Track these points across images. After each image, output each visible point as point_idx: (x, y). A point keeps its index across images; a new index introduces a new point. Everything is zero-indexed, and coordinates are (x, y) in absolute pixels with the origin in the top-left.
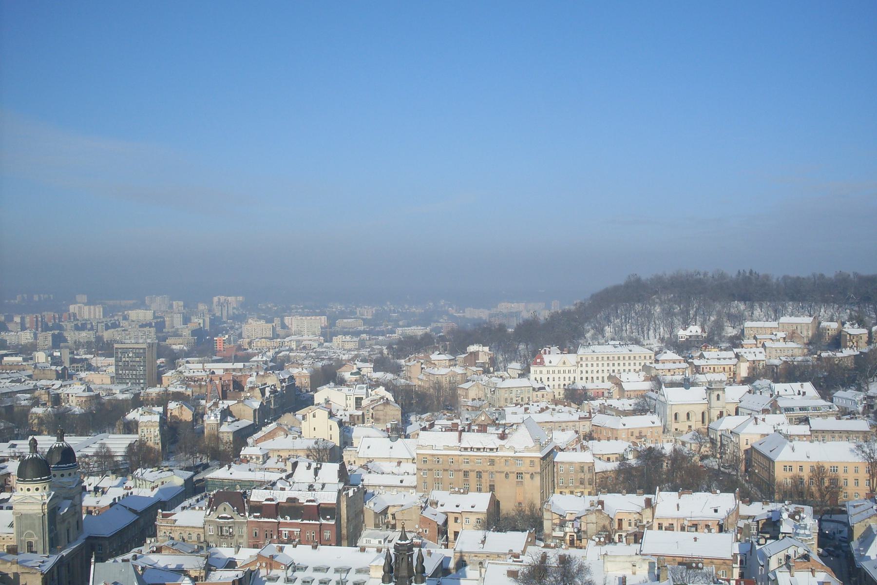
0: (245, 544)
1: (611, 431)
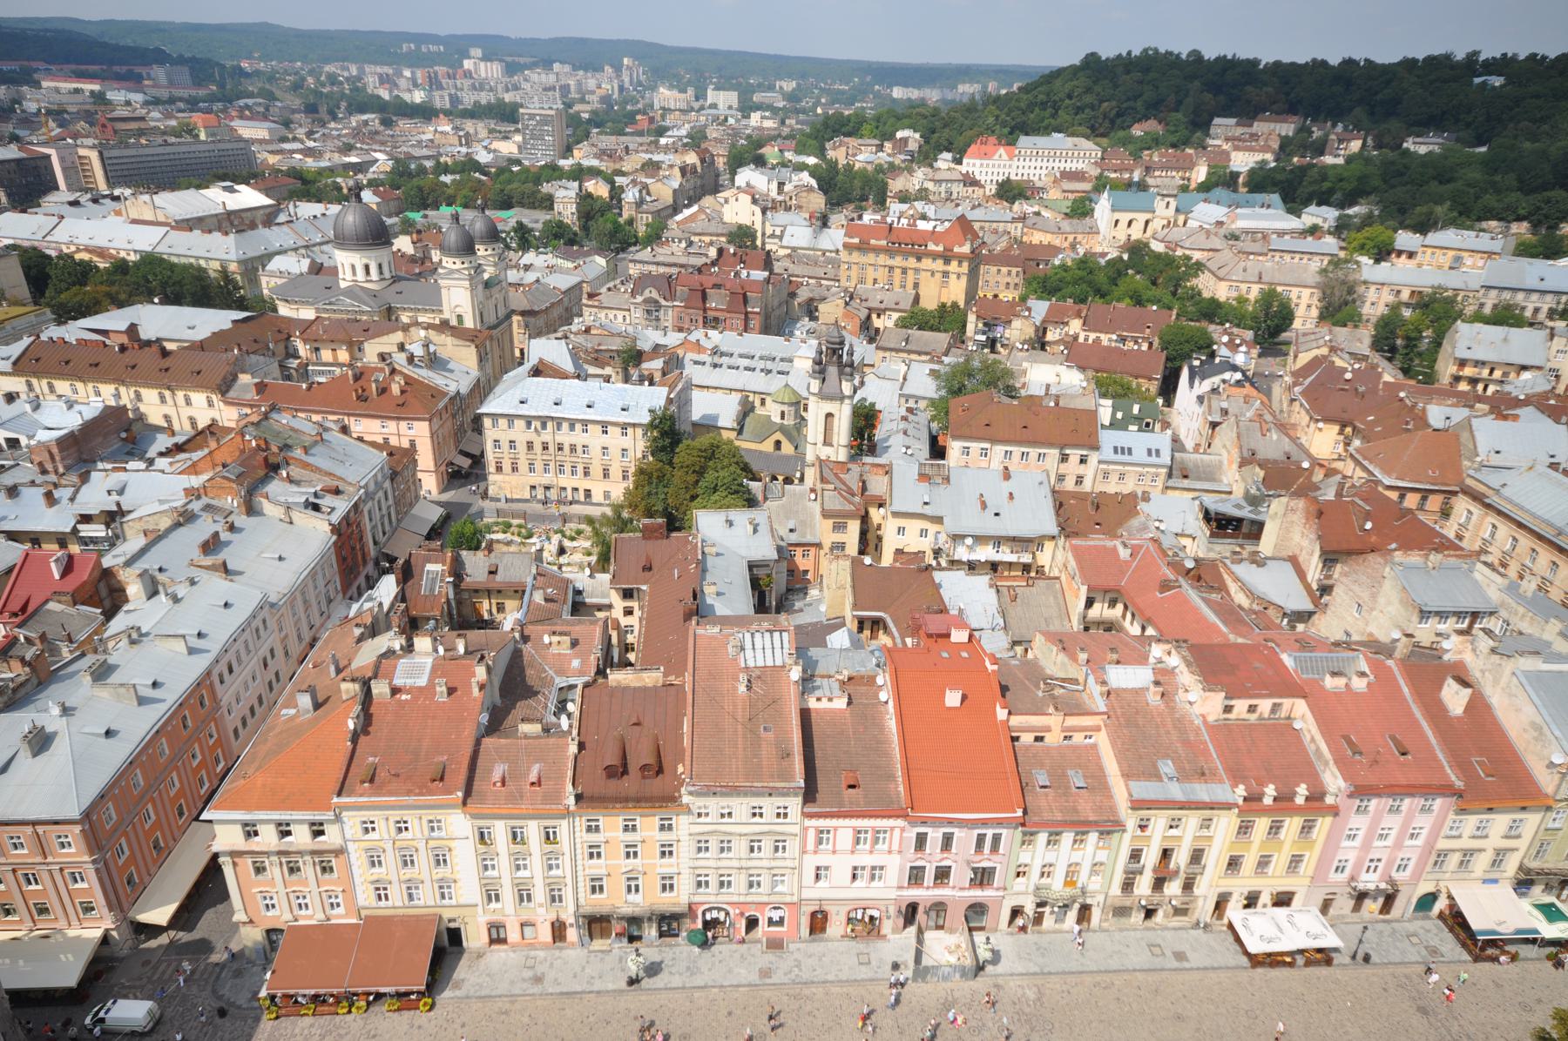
0: (670, 328)
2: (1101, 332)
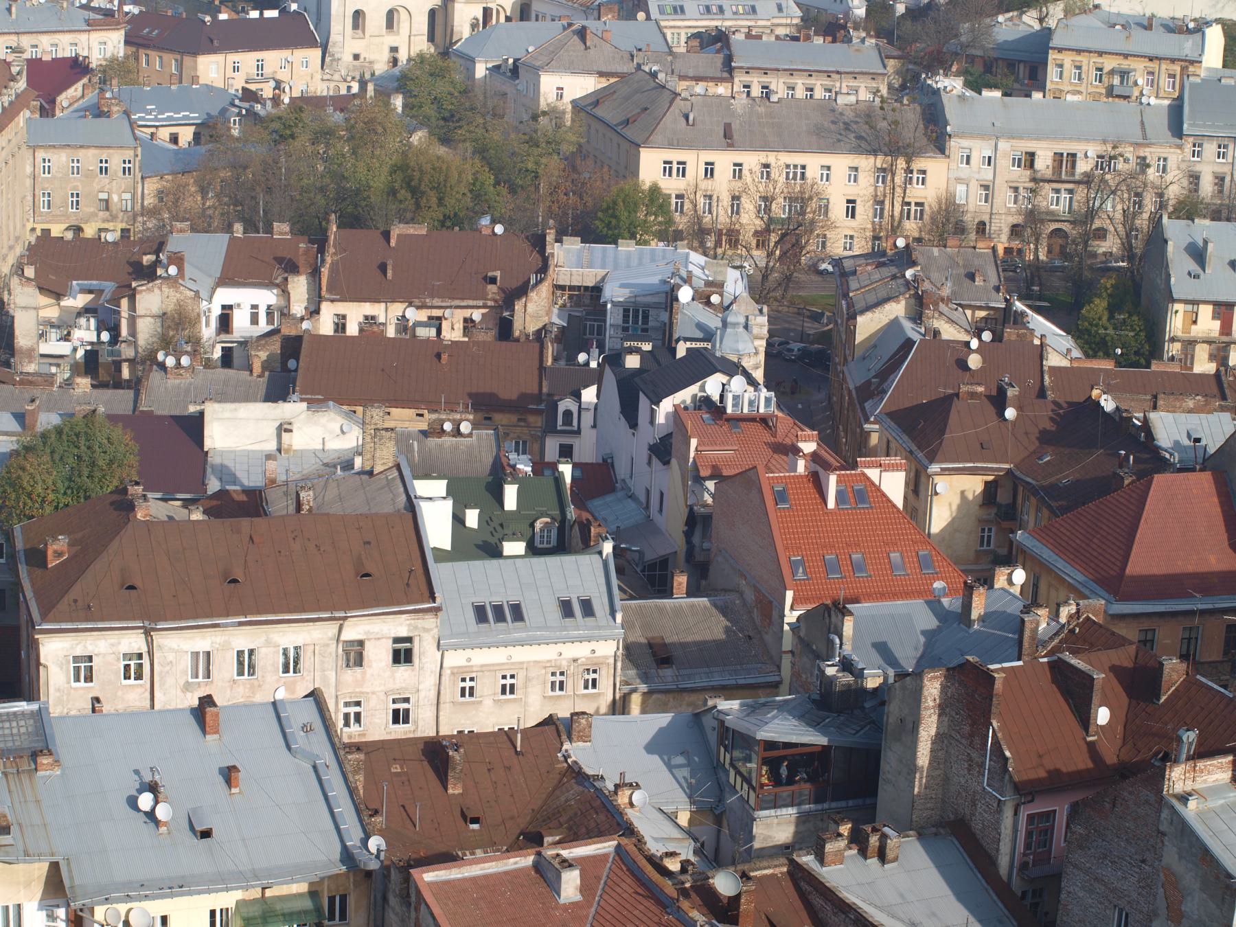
1: (176, 60)
2: (375, 300)
